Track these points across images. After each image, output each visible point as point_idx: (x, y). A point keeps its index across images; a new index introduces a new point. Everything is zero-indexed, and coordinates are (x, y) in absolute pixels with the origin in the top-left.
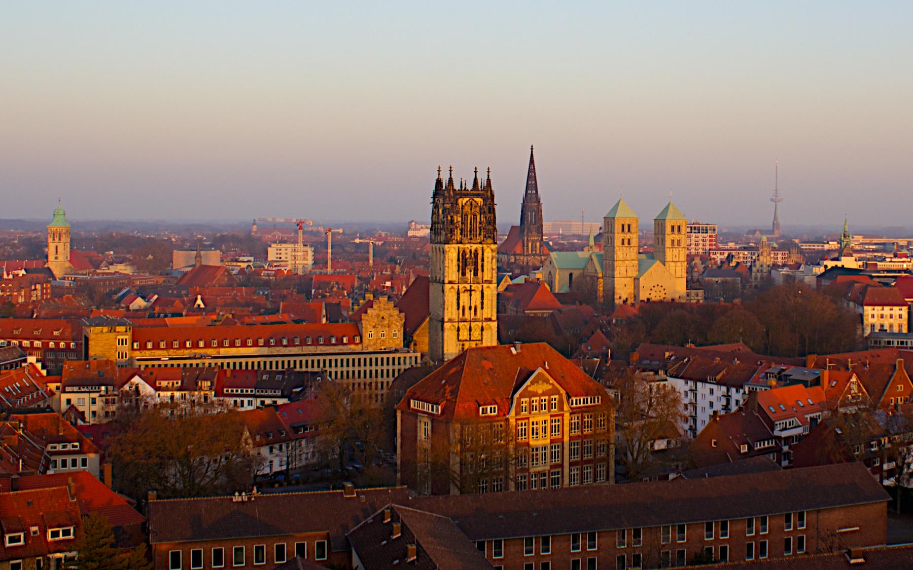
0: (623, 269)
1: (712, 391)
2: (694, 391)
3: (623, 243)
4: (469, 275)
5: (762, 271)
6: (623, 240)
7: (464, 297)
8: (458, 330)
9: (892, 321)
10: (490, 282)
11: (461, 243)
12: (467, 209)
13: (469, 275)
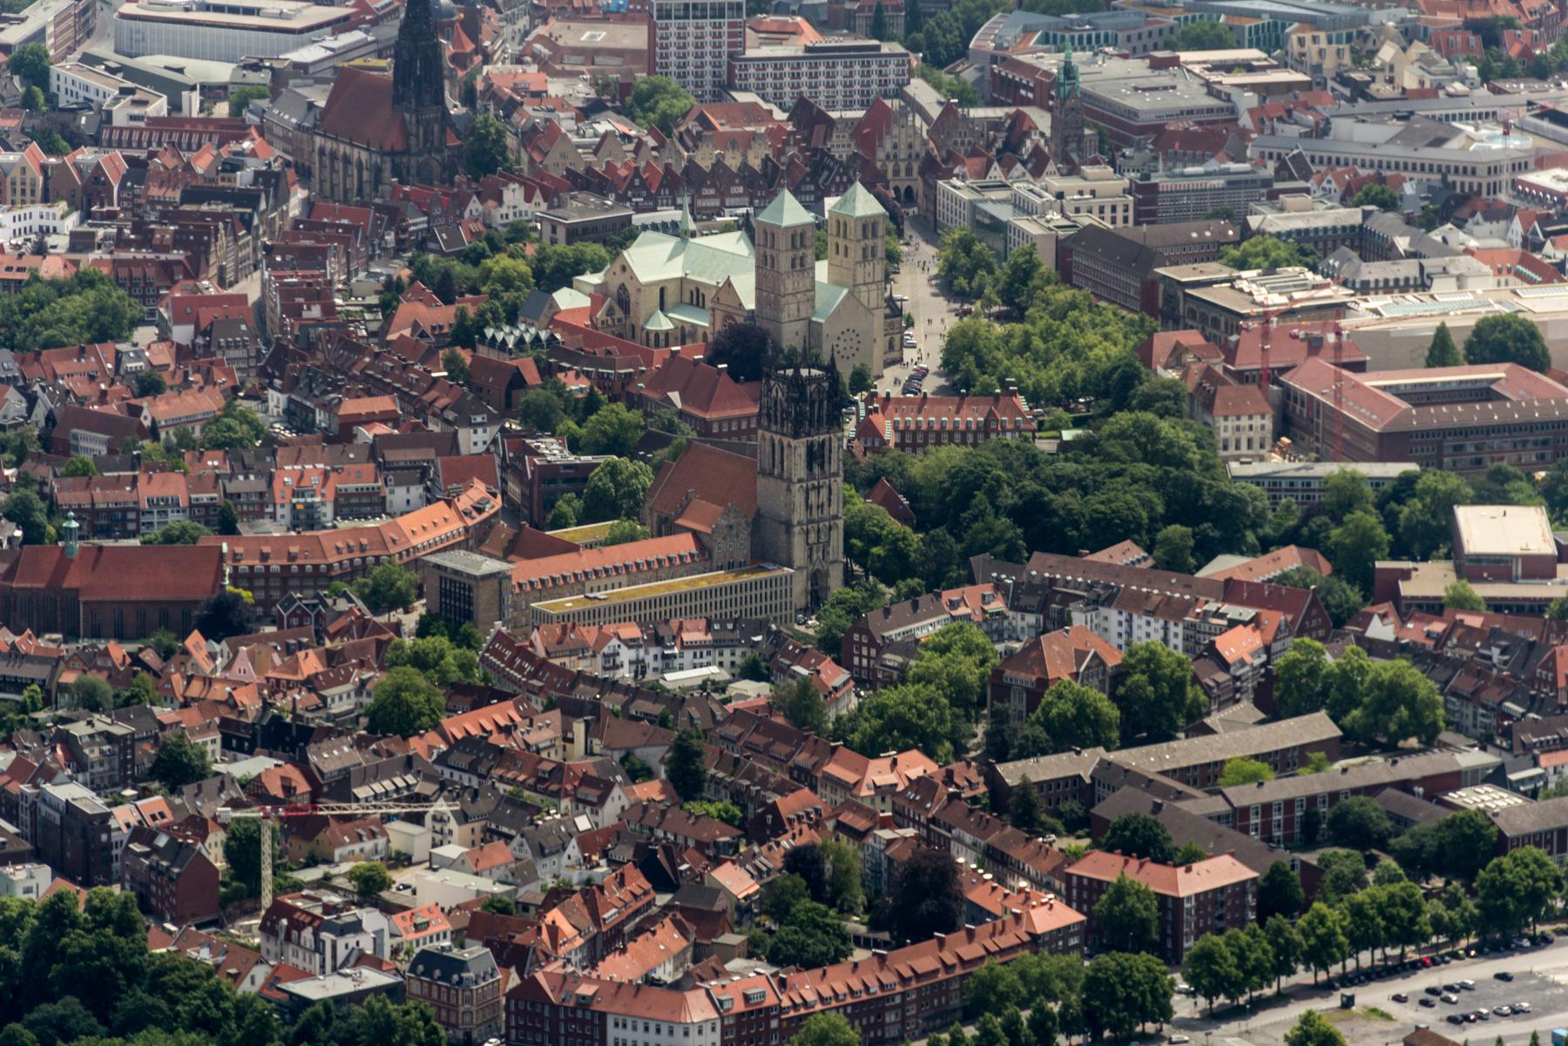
0: (793, 307)
1: (1148, 623)
2: (1129, 620)
3: (793, 266)
4: (816, 470)
5: (895, 156)
6: (793, 260)
7: (813, 496)
8: (808, 532)
9: (1251, 434)
10: (836, 475)
11: (809, 435)
12: (815, 396)
13: (816, 470)
